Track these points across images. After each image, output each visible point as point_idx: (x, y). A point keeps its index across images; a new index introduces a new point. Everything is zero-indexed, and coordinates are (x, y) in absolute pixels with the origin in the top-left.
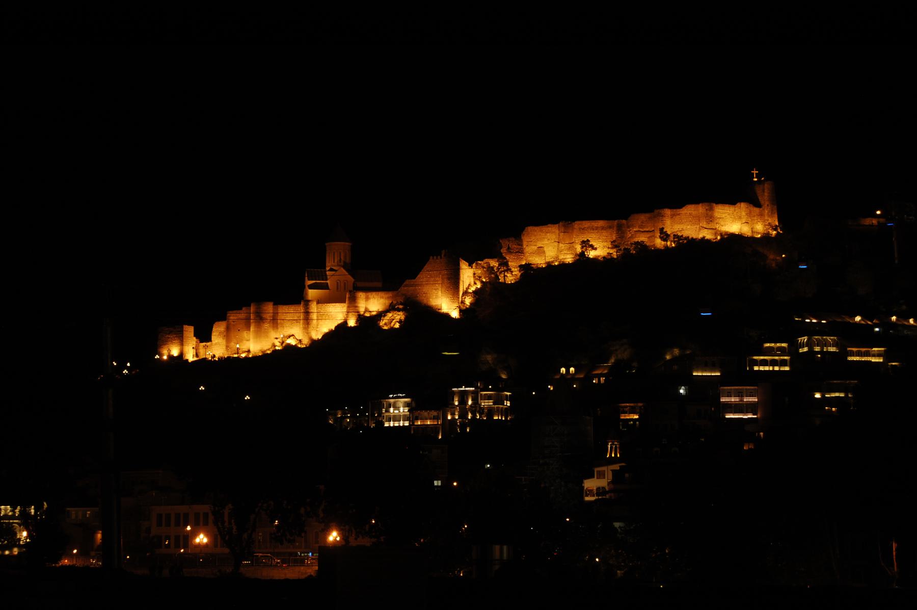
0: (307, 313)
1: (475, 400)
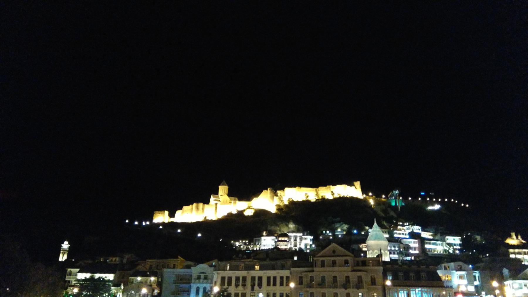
0: (216, 208)
1: (301, 239)
